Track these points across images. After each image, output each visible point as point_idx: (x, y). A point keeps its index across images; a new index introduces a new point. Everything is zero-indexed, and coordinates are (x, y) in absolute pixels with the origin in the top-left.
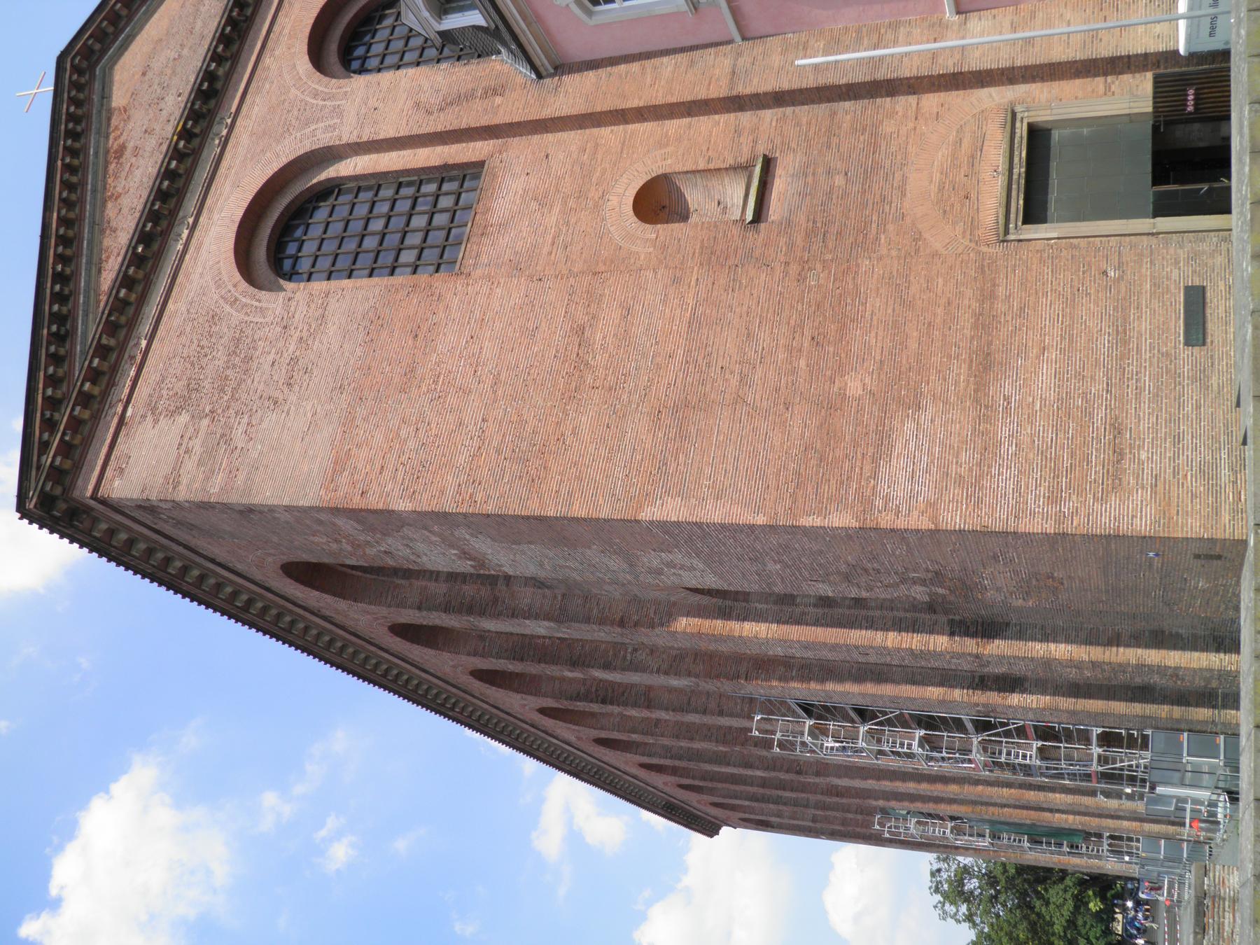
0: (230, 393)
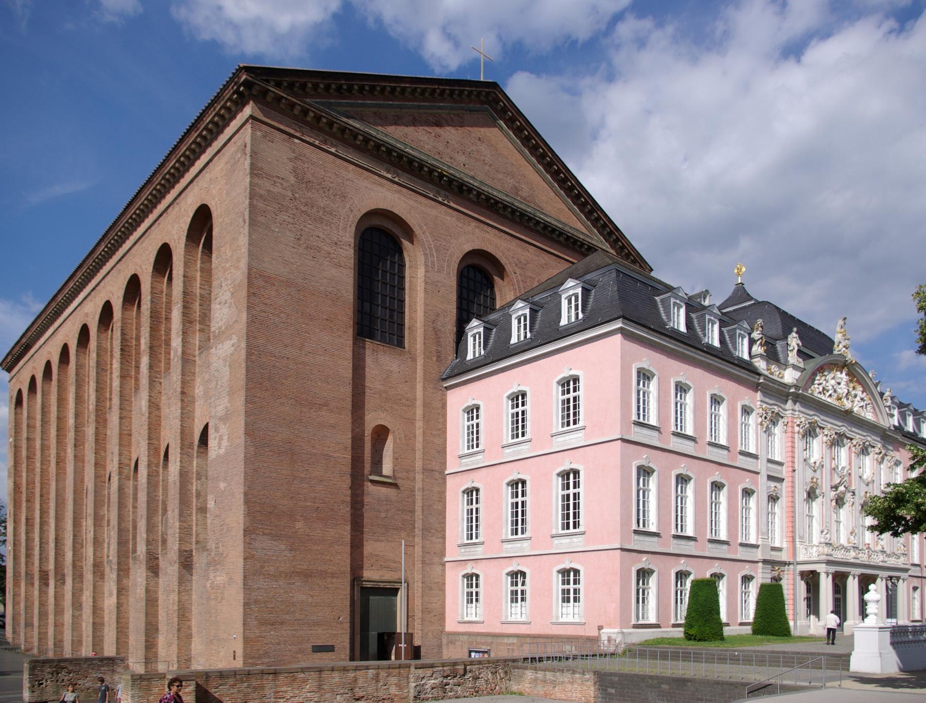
0: (304, 209)
